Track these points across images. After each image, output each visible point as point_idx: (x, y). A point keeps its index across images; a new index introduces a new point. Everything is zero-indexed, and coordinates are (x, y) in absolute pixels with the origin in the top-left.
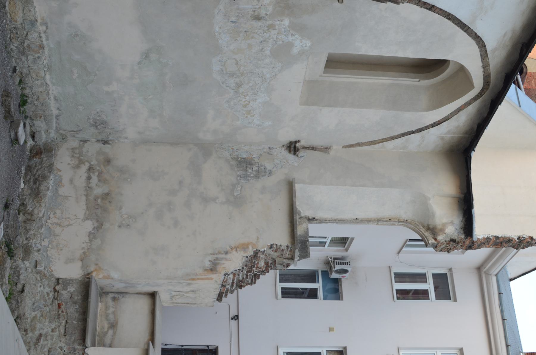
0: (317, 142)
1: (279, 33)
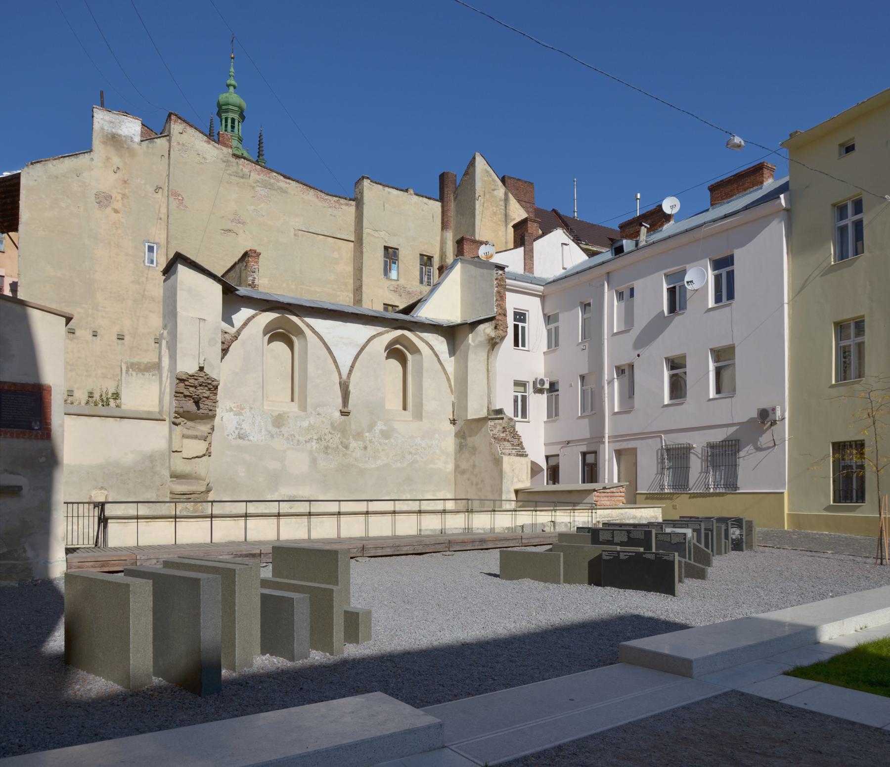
1: (374, 437)
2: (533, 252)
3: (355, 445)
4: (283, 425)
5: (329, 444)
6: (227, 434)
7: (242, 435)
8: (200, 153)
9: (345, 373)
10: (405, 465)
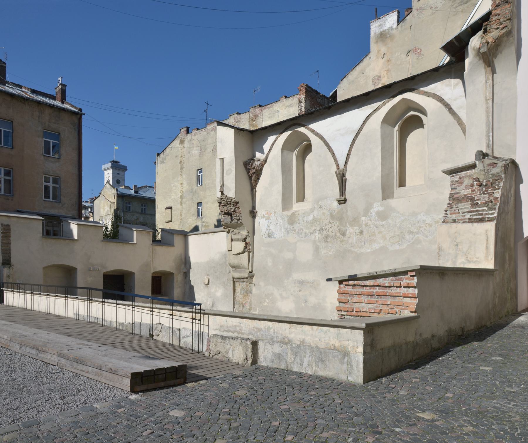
1: (371, 220)
3: (352, 231)
5: (329, 233)
6: (262, 234)
7: (270, 234)
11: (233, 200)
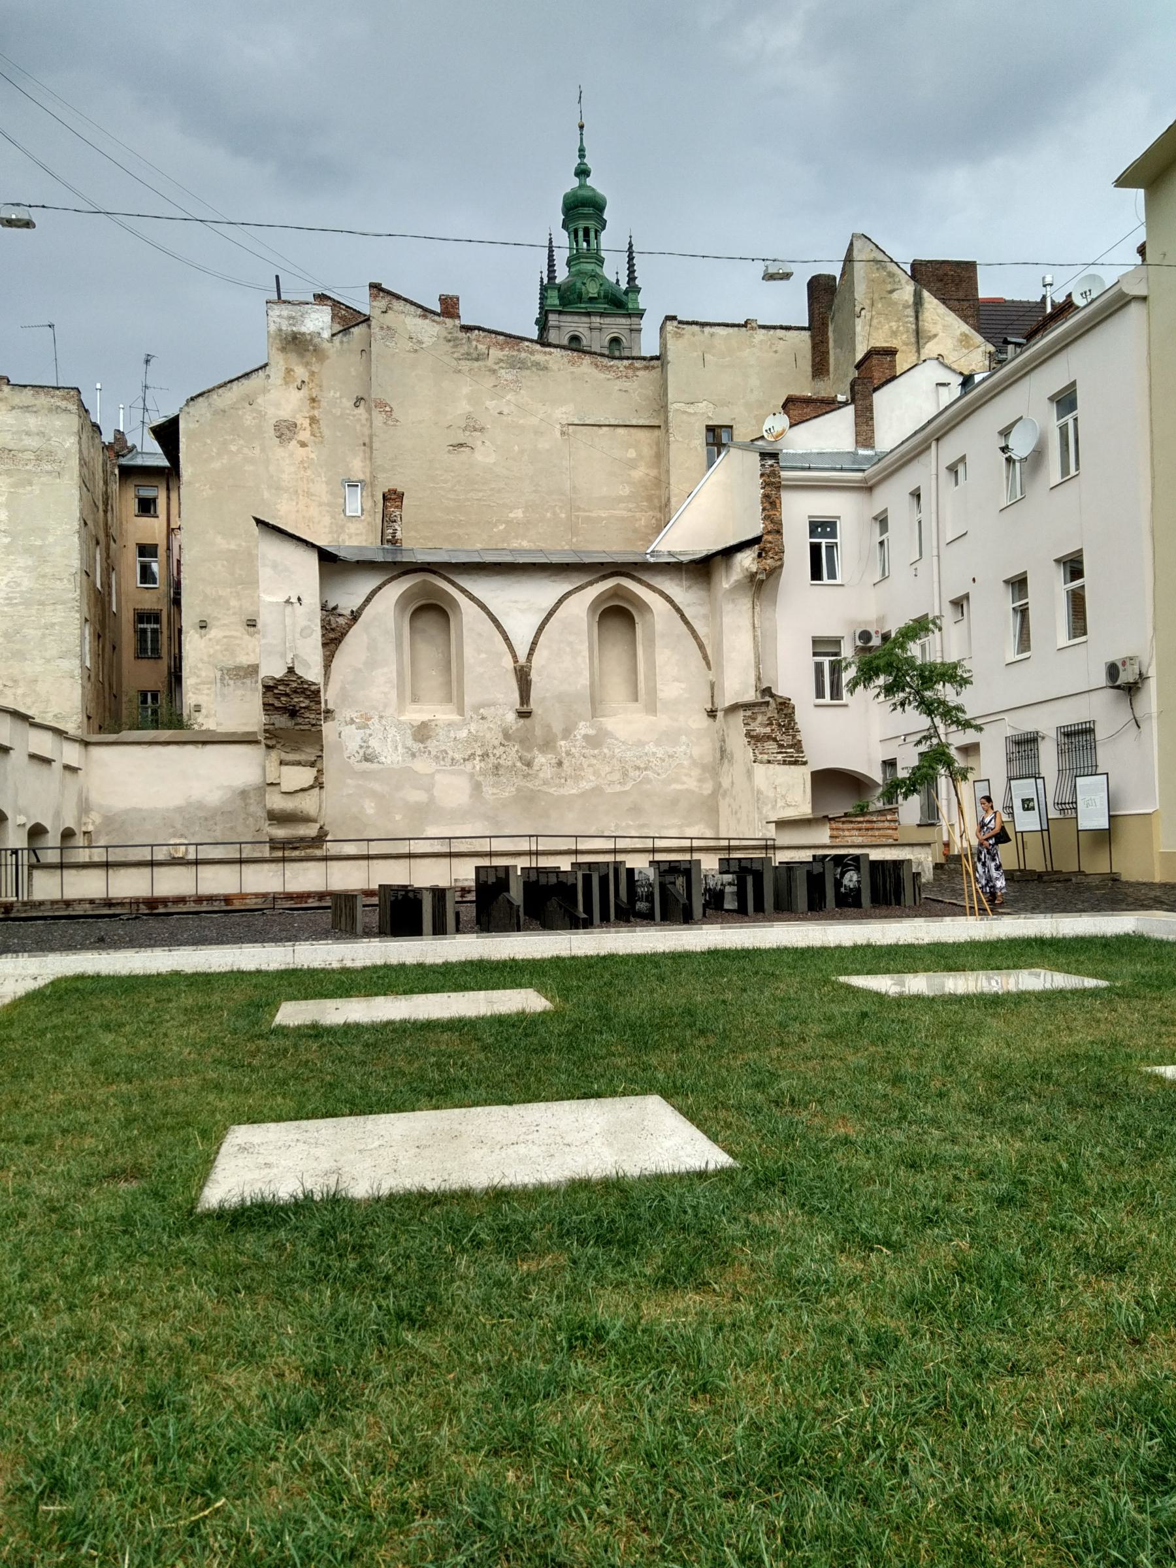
0: (707, 693)
2: (871, 411)
3: (543, 760)
4: (429, 737)
5: (502, 761)
8: (413, 335)
9: (522, 652)
10: (627, 788)
11: (313, 688)
